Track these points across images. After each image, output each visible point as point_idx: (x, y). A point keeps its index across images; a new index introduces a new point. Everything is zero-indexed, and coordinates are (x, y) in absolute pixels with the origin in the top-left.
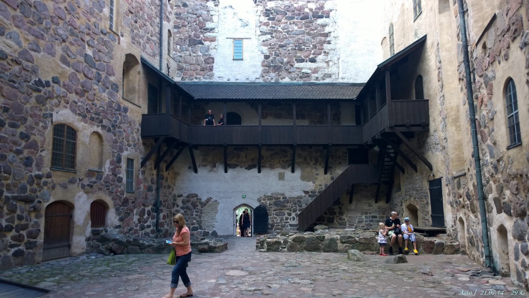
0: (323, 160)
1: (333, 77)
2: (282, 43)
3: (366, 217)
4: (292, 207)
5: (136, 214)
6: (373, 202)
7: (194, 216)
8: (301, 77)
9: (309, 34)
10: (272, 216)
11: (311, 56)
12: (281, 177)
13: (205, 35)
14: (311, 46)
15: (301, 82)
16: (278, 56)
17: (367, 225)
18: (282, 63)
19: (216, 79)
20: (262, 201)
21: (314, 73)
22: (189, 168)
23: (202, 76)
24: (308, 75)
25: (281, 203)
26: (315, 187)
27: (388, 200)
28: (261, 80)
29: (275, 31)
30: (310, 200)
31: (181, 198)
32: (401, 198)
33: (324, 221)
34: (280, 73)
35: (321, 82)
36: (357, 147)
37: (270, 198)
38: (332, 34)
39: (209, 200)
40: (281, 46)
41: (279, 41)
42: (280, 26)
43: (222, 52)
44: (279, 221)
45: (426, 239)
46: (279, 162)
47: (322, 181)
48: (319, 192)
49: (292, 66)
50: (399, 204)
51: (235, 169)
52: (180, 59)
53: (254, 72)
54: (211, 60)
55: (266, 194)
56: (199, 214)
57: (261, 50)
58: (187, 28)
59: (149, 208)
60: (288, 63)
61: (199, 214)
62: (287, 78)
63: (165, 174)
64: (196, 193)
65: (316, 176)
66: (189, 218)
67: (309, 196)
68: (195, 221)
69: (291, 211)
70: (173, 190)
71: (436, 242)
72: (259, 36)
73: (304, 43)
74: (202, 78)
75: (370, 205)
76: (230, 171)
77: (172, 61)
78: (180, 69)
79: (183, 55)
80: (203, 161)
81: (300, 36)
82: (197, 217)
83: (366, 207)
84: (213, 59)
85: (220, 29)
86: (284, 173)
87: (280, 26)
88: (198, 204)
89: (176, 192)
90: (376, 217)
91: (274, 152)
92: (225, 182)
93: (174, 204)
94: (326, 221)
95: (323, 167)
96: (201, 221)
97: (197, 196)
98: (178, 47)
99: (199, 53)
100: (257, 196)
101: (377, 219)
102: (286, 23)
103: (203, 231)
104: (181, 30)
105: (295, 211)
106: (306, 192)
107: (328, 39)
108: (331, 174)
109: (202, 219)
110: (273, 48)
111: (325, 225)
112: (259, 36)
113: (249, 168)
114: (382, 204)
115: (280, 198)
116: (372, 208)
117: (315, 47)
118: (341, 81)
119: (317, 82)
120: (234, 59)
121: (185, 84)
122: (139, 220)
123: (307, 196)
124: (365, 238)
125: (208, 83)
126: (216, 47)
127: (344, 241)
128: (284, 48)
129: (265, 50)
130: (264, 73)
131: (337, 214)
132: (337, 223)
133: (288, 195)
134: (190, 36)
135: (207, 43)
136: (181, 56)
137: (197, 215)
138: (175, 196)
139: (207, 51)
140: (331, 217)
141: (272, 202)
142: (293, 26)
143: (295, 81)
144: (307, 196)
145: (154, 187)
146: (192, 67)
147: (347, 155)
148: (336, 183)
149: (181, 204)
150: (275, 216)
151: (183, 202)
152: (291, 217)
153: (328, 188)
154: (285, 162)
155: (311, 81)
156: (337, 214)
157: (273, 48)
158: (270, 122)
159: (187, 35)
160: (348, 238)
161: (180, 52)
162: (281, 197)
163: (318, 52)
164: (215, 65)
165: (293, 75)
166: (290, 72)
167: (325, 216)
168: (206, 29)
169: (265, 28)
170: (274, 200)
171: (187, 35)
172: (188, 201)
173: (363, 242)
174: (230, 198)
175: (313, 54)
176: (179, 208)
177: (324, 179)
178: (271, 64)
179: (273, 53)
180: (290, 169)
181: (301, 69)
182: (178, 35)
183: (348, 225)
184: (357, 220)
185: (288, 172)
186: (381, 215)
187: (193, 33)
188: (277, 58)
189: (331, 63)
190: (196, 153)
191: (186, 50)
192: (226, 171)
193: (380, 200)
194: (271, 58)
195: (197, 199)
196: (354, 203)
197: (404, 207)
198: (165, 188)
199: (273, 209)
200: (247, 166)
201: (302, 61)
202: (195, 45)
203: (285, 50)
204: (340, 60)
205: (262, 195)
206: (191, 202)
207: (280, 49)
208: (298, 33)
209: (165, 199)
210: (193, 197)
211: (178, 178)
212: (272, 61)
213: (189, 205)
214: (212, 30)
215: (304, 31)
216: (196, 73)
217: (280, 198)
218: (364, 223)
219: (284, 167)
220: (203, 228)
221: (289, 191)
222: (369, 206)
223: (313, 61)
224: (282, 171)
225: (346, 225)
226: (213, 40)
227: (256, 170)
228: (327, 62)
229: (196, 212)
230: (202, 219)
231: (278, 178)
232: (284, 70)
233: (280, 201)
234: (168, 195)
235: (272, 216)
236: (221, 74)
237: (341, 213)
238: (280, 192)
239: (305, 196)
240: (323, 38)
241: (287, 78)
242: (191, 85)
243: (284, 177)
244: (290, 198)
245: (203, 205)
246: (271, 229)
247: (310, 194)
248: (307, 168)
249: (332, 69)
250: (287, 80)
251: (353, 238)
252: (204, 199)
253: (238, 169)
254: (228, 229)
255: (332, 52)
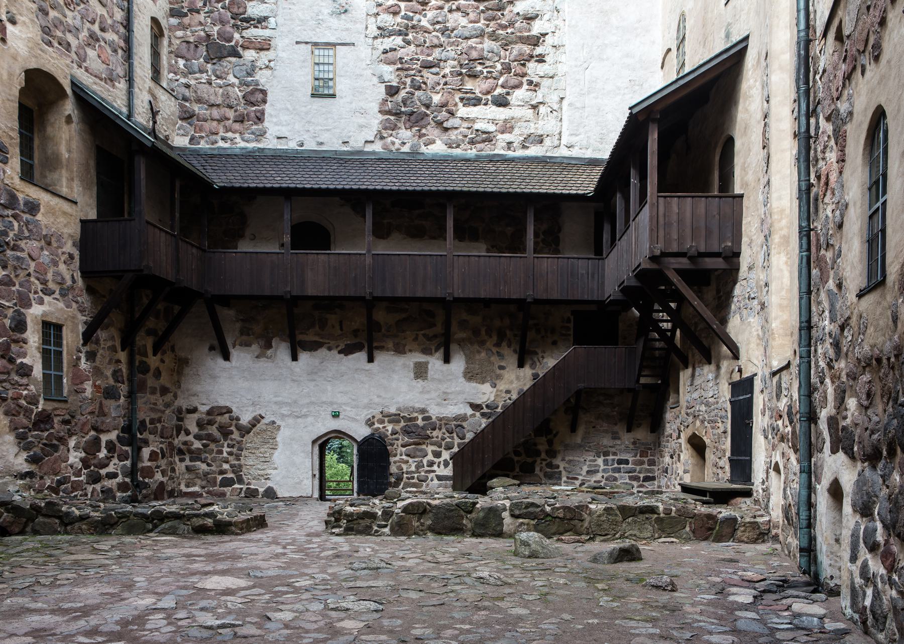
0: (515, 336)
1: (547, 142)
2: (430, 58)
3: (606, 462)
4: (443, 439)
5: (76, 448)
6: (620, 429)
7: (225, 455)
8: (472, 142)
9: (493, 36)
10: (397, 458)
11: (499, 91)
12: (420, 372)
13: (246, 33)
14: (499, 67)
15: (472, 152)
16: (419, 88)
17: (607, 479)
18: (428, 106)
19: (270, 143)
20: (377, 425)
21: (502, 133)
22: (212, 348)
23: (237, 135)
24: (488, 138)
25: (418, 430)
26: (496, 396)
27: (656, 425)
28: (377, 147)
29: (413, 27)
30: (484, 422)
31: (196, 416)
32: (678, 421)
33: (513, 470)
34: (424, 131)
35: (520, 153)
36: (593, 308)
37: (394, 418)
38: (549, 40)
39: (257, 420)
40: (428, 66)
41: (422, 53)
42: (425, 16)
43: (285, 74)
44: (413, 468)
45: (703, 509)
46: (416, 339)
47: (512, 382)
48: (503, 406)
49: (452, 114)
50: (675, 435)
51: (314, 353)
52: (187, 93)
53: (361, 126)
54: (260, 96)
55: (386, 410)
56: (235, 450)
57: (378, 73)
58: (201, 17)
59: (113, 436)
60: (443, 105)
61: (235, 450)
62: (438, 142)
63: (153, 361)
64: (228, 404)
65: (498, 372)
66: (214, 460)
67: (483, 415)
68: (226, 466)
69: (440, 446)
70: (175, 396)
71: (720, 516)
72: (375, 38)
73: (481, 59)
74: (238, 140)
75: (615, 437)
76: (304, 356)
77: (163, 97)
78: (187, 117)
79: (192, 82)
80: (242, 334)
81: (471, 42)
82: (231, 458)
83: (606, 441)
84: (264, 92)
85: (280, 20)
86: (427, 363)
87: (425, 16)
88: (233, 428)
89: (183, 403)
90: (626, 462)
91: (404, 316)
92: (293, 380)
93: (179, 429)
94: (517, 470)
95: (515, 351)
96: (240, 466)
97: (229, 411)
98: (181, 62)
99: (232, 79)
100: (365, 414)
101: (630, 466)
102: (441, 8)
103: (244, 487)
104: (186, 20)
105: (448, 448)
106: (475, 407)
107: (539, 50)
108: (533, 366)
109: (242, 462)
110: (407, 70)
111: (514, 478)
112: (375, 38)
113: (347, 351)
114: (641, 434)
115: (416, 419)
116: (619, 442)
117: (507, 69)
118: (564, 152)
119: (510, 154)
120: (313, 96)
121: (197, 153)
122: (85, 463)
123: (478, 414)
124: (565, 508)
125: (253, 151)
126: (272, 64)
127: (517, 512)
128: (434, 70)
129: (389, 72)
130: (385, 129)
131: (543, 455)
132: (541, 475)
133: (435, 412)
134: (208, 36)
135: (249, 55)
136: (188, 86)
137: (230, 454)
138: (180, 410)
139: (249, 74)
140: (529, 460)
141: (398, 428)
142: (457, 15)
143: (457, 152)
144: (478, 414)
145: (124, 389)
146: (215, 113)
147: (571, 325)
148: (539, 386)
149: (194, 429)
150: (404, 457)
151: (200, 425)
152: (441, 459)
153: (523, 395)
154: (429, 338)
155: (496, 152)
156: (543, 455)
157: (407, 70)
158: (395, 248)
159: (202, 33)
160: (527, 507)
161: (185, 76)
162: (420, 417)
163: (514, 81)
164: (268, 108)
165: (453, 135)
166: (446, 130)
167: (516, 459)
168: (248, 20)
169: (387, 20)
170: (402, 424)
171: (202, 33)
172: (211, 423)
173: (561, 515)
174: (306, 416)
175: (503, 86)
176: (191, 438)
177: (518, 378)
178: (402, 110)
179: (408, 80)
180: (440, 354)
181: (473, 121)
182: (180, 33)
183: (564, 479)
184: (585, 468)
185: (435, 363)
186: (638, 457)
187: (216, 29)
188: (417, 93)
189: (542, 109)
190: (226, 314)
191: (201, 72)
192: (295, 358)
193: (639, 426)
194: (403, 94)
195: (231, 419)
196: (581, 431)
197: (683, 440)
198: (153, 392)
199: (400, 442)
200: (342, 346)
201: (477, 102)
202: (220, 58)
203: (437, 74)
204: (565, 102)
205: (376, 412)
206: (216, 425)
207: (425, 73)
208: (467, 34)
209: (155, 416)
210: (222, 414)
211: (187, 370)
212: (404, 102)
213: (213, 430)
214: (261, 21)
215: (483, 30)
216: (225, 127)
217: (416, 419)
218: (600, 475)
219: (427, 351)
220: (246, 481)
221: (438, 405)
222: (614, 438)
223: (501, 102)
224: (421, 358)
225: (561, 479)
226: (264, 46)
227: (362, 356)
228: (534, 107)
229: (228, 446)
230: (242, 462)
231: (412, 375)
232: (433, 124)
233: (417, 426)
234: (161, 407)
235: (397, 458)
236: (284, 131)
237: (552, 454)
238: (417, 405)
239: (473, 415)
240: (526, 49)
241: (438, 142)
242: (212, 156)
243: (426, 372)
244: (440, 419)
245: (245, 431)
246: (396, 484)
247: (485, 410)
248: (479, 352)
249: (546, 125)
250: (438, 148)
251: (538, 506)
252: (245, 419)
253: (323, 352)
254: (300, 483)
255: (545, 83)
